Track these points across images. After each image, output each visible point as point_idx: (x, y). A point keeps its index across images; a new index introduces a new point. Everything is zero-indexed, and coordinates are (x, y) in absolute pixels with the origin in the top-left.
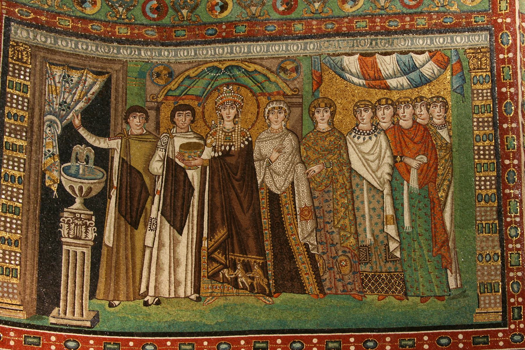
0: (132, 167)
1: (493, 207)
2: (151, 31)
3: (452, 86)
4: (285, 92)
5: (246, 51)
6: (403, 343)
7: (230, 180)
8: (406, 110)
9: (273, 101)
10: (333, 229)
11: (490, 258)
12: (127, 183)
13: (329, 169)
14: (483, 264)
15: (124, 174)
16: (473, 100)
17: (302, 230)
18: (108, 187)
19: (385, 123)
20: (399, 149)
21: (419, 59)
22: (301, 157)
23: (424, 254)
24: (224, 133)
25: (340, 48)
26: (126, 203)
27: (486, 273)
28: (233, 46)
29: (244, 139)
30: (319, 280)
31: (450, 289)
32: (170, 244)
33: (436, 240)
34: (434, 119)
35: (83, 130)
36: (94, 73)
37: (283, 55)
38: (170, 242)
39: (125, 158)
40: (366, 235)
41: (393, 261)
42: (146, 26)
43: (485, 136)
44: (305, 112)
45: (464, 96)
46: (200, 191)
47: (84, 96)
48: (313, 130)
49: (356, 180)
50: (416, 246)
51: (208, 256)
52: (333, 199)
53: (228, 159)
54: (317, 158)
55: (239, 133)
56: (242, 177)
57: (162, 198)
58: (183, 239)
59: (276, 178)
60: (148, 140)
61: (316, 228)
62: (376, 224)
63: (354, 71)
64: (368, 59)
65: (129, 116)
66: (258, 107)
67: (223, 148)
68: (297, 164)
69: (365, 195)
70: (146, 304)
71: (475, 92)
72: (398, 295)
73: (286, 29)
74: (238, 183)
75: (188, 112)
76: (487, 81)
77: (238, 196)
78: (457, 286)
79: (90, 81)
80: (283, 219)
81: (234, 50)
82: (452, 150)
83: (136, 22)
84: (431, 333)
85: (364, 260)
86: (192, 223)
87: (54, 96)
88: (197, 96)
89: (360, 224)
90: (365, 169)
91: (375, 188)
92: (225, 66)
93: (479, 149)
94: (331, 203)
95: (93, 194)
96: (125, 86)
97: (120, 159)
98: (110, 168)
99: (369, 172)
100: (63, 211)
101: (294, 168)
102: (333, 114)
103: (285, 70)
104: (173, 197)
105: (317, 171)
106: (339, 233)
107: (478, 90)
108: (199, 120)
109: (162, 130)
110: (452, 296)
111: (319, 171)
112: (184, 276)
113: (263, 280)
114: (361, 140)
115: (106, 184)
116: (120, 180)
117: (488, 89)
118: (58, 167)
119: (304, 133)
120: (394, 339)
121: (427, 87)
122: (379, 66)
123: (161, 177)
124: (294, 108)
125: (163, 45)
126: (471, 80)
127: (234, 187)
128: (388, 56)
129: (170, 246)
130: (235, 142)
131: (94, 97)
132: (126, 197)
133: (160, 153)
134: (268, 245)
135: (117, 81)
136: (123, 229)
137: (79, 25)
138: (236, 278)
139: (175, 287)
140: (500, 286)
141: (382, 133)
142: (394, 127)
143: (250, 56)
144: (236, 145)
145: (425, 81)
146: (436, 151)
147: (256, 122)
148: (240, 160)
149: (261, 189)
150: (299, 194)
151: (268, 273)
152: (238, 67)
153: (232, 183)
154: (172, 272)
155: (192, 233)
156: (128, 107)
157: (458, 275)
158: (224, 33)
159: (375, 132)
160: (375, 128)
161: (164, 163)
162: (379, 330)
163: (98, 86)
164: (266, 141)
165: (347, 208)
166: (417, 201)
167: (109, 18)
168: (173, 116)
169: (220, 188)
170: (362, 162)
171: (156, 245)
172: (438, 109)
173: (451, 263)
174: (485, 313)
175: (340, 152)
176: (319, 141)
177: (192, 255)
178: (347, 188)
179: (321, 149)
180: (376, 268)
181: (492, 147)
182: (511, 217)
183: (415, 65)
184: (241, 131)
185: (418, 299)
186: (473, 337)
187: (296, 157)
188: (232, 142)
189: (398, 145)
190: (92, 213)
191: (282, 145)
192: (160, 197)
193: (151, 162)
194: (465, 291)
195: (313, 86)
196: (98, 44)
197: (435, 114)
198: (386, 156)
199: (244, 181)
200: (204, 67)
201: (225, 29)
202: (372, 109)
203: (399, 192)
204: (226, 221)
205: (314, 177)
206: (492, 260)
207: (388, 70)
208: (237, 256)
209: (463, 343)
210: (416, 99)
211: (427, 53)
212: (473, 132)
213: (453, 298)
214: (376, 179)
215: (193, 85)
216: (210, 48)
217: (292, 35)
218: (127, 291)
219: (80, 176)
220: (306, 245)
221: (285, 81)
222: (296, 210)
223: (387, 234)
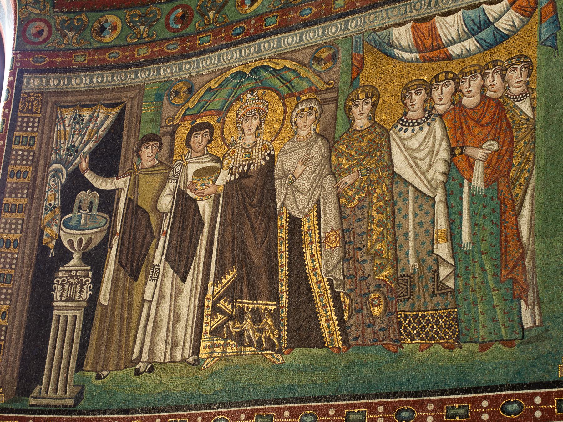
4: (317, 88)
5: (275, 46)
6: (454, 411)
7: (245, 207)
8: (472, 83)
9: (302, 102)
12: (131, 226)
13: (365, 178)
15: (130, 215)
19: (442, 104)
20: (459, 137)
22: (331, 167)
24: (243, 151)
25: (389, 18)
32: (171, 295)
34: (511, 88)
37: (319, 42)
38: (172, 293)
39: (132, 198)
40: (408, 261)
41: (444, 293)
42: (168, 40)
44: (341, 107)
45: (556, 49)
48: (349, 129)
52: (368, 216)
53: (245, 182)
54: (351, 166)
57: (167, 240)
58: (187, 287)
59: (299, 197)
62: (423, 243)
63: (404, 43)
65: (141, 147)
67: (241, 169)
68: (325, 177)
70: (138, 373)
72: (447, 342)
73: (325, 9)
75: (205, 131)
80: (304, 250)
81: (262, 48)
82: (535, 128)
84: (493, 396)
86: (198, 267)
89: (401, 246)
90: (411, 171)
92: (250, 69)
94: (364, 222)
96: (139, 114)
97: (126, 199)
98: (114, 211)
99: (417, 175)
101: (321, 184)
106: (373, 260)
111: (352, 181)
112: (183, 332)
113: (273, 333)
114: (409, 133)
119: (337, 136)
121: (504, 45)
122: (439, 31)
123: (169, 213)
129: (171, 298)
130: (255, 159)
133: (171, 185)
134: (283, 288)
135: (131, 110)
138: (241, 334)
139: (171, 349)
141: (437, 119)
142: (454, 109)
147: (280, 130)
151: (280, 323)
152: (265, 68)
153: (247, 212)
154: (171, 328)
158: (253, 29)
159: (428, 119)
160: (428, 114)
161: (174, 197)
164: (290, 153)
167: (129, 40)
170: (409, 163)
171: (155, 299)
172: (517, 73)
175: (381, 153)
177: (194, 306)
179: (356, 153)
185: (475, 347)
189: (459, 132)
195: (352, 73)
197: (514, 81)
198: (441, 149)
201: (254, 25)
202: (426, 90)
207: (450, 34)
210: (487, 64)
215: (213, 97)
216: (235, 51)
217: (331, 15)
221: (318, 74)
222: (320, 238)
223: (437, 255)
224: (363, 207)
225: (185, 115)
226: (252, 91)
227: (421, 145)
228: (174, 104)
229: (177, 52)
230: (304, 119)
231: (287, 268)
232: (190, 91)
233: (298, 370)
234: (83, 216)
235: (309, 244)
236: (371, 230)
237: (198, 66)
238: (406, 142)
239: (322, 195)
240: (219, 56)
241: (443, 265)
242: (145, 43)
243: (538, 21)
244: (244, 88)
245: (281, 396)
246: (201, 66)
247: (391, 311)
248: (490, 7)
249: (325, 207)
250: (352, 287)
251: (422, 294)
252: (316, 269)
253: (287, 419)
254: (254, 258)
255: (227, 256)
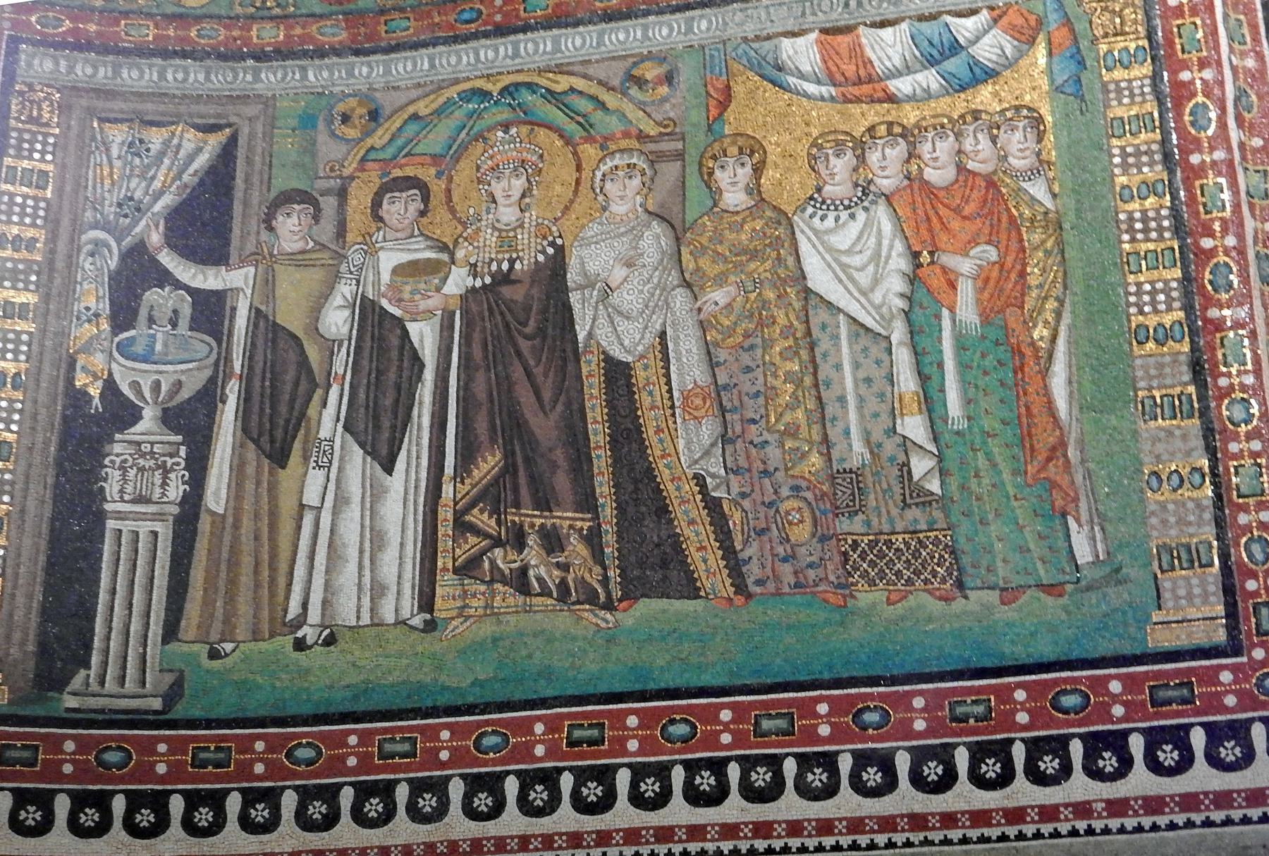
0: (278, 325)
1: (1179, 353)
2: (332, 26)
3: (1052, 81)
5: (549, 48)
6: (960, 710)
9: (613, 153)
10: (767, 436)
11: (1182, 481)
12: (265, 363)
13: (753, 296)
14: (1162, 498)
15: (260, 342)
16: (1107, 106)
17: (689, 443)
18: (221, 375)
21: (965, 27)
22: (682, 273)
23: (1003, 484)
24: (496, 234)
26: (262, 410)
27: (1172, 520)
28: (518, 42)
29: (545, 243)
30: (732, 562)
31: (1077, 565)
32: (363, 497)
33: (1032, 447)
35: (168, 254)
36: (198, 128)
37: (637, 51)
39: (263, 308)
41: (924, 503)
42: (321, 16)
43: (1144, 187)
44: (692, 170)
45: (1083, 99)
46: (438, 367)
47: (173, 180)
49: (819, 317)
50: (981, 461)
51: (455, 520)
52: (764, 364)
53: (506, 291)
54: (722, 273)
55: (533, 229)
56: (539, 328)
59: (623, 325)
60: (318, 263)
61: (723, 436)
62: (876, 415)
63: (805, 68)
64: (840, 38)
66: (579, 168)
69: (845, 349)
70: (300, 645)
71: (1112, 87)
72: (939, 589)
74: (530, 343)
76: (1140, 59)
77: (529, 374)
78: (1098, 556)
79: (188, 146)
80: (641, 421)
81: (522, 50)
83: (298, 12)
84: (1034, 681)
85: (848, 506)
87: (107, 187)
88: (434, 156)
89: (834, 419)
91: (868, 330)
92: (500, 86)
93: (1131, 219)
94: (759, 373)
95: (185, 394)
98: (226, 332)
99: (851, 294)
100: (112, 441)
102: (758, 170)
103: (640, 82)
104: (372, 388)
105: (722, 302)
106: (781, 444)
107: (1117, 83)
108: (438, 209)
109: (350, 237)
110: (1083, 583)
113: (590, 570)
114: (830, 222)
115: (216, 371)
116: (250, 358)
117: (1145, 77)
118: (105, 343)
119: (690, 217)
120: (935, 701)
123: (346, 343)
124: (663, 165)
125: (357, 53)
126: (1099, 62)
127: (519, 354)
128: (890, 30)
131: (196, 180)
132: (262, 396)
133: (345, 290)
134: (603, 487)
136: (250, 470)
137: (171, 32)
138: (524, 571)
139: (372, 599)
140: (1215, 551)
141: (880, 201)
143: (559, 58)
144: (526, 257)
145: (983, 75)
146: (1020, 234)
148: (534, 291)
149: (585, 352)
150: (679, 360)
151: (603, 552)
152: (530, 86)
153: (515, 345)
154: (367, 562)
155: (418, 465)
156: (273, 194)
157: (1097, 528)
161: (353, 312)
162: (893, 681)
163: (207, 156)
164: (596, 243)
165: (799, 383)
166: (978, 354)
167: (239, 10)
168: (377, 204)
169: (486, 357)
171: (329, 503)
173: (1076, 500)
174: (1178, 622)
175: (779, 254)
176: (727, 232)
177: (415, 520)
178: (799, 335)
179: (730, 251)
180: (880, 523)
181: (1164, 212)
182: (1229, 375)
183: (956, 40)
184: (538, 224)
185: (994, 596)
186: (1151, 688)
187: (669, 275)
188: (517, 251)
190: (179, 438)
191: (636, 248)
192: (342, 390)
193: (323, 311)
194: (1118, 570)
195: (708, 110)
196: (210, 67)
199: (544, 339)
200: (452, 93)
201: (501, 7)
203: (930, 335)
204: (499, 433)
205: (715, 317)
206: (1187, 485)
208: (528, 516)
209: (1125, 704)
211: (985, 12)
212: (1113, 181)
213: (1089, 588)
214: (870, 308)
218: (255, 617)
219: (156, 358)
220: (700, 480)
221: (641, 106)
222: (671, 398)
223: (904, 437)
224: (752, 347)
225: (363, 160)
226: (506, 127)
227: (854, 244)
228: (342, 139)
229: (340, 42)
230: (618, 185)
231: (609, 453)
232: (374, 115)
233: (650, 639)
234: (159, 335)
235: (651, 409)
236: (773, 388)
237: (388, 72)
238: (826, 238)
239: (669, 322)
240: (432, 60)
241: (918, 454)
242: (271, 18)
243: (1044, 52)
244: (488, 120)
245: (618, 687)
246: (394, 72)
247: (826, 532)
248: (958, 20)
249: (676, 344)
250: (743, 489)
251: (882, 503)
252: (669, 455)
253: (634, 729)
254: (537, 431)
255: (481, 427)
